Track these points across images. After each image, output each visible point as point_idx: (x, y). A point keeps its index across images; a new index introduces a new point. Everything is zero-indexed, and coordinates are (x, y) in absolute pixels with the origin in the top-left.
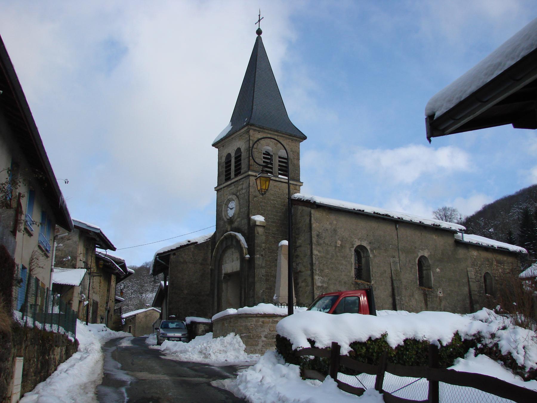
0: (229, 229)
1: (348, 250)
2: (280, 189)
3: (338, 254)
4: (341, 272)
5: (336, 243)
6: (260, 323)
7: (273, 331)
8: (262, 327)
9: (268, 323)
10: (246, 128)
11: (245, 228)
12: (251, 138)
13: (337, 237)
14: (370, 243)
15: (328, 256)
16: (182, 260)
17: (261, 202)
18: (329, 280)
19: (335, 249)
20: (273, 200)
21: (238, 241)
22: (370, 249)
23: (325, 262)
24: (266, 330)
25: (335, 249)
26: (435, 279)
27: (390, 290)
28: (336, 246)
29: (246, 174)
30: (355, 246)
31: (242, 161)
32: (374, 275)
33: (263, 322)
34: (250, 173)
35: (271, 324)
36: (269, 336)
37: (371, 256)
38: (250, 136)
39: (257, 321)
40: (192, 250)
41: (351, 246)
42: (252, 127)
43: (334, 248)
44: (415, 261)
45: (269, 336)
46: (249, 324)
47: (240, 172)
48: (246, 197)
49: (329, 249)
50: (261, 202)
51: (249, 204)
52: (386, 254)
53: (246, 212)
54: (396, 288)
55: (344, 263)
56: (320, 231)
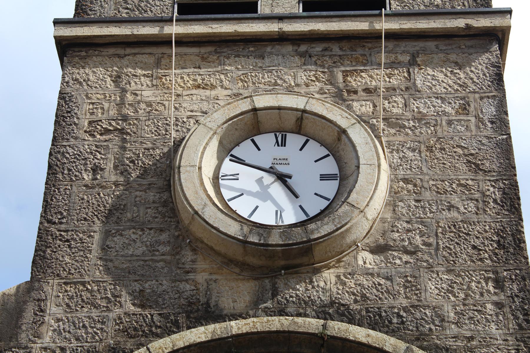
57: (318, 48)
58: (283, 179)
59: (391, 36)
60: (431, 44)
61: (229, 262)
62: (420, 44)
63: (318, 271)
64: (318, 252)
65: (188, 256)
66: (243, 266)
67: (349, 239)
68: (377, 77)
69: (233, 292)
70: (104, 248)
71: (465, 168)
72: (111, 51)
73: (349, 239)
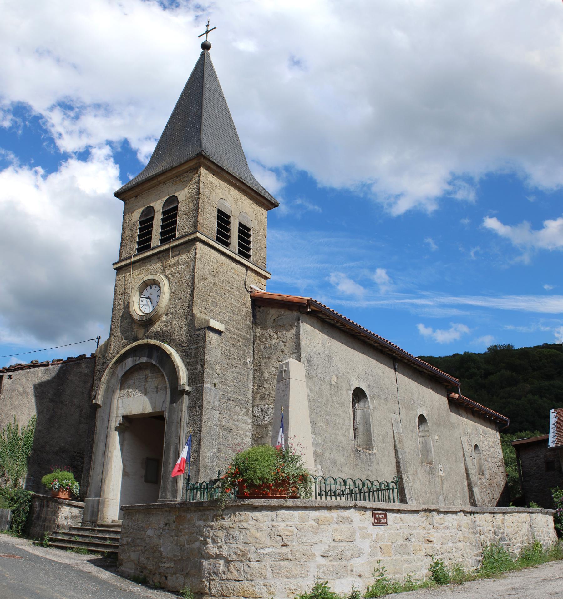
0: (140, 335)
1: (345, 392)
2: (238, 275)
3: (334, 398)
4: (339, 429)
5: (331, 378)
6: (312, 522)
7: (340, 541)
8: (316, 533)
13: (332, 369)
14: (369, 386)
15: (321, 400)
16: (21, 389)
17: (211, 290)
18: (324, 441)
19: (331, 388)
20: (229, 292)
21: (168, 357)
22: (370, 396)
23: (318, 410)
24: (324, 539)
25: (331, 388)
27: (394, 464)
28: (331, 385)
29: (192, 237)
30: (353, 388)
31: (178, 218)
32: (375, 439)
33: (318, 521)
34: (199, 235)
35: (335, 526)
36: (333, 553)
37: (371, 407)
38: (199, 177)
40: (40, 375)
41: (348, 387)
42: (206, 162)
43: (328, 387)
44: (415, 422)
45: (333, 553)
46: (282, 525)
47: (175, 236)
48: (187, 276)
49: (323, 387)
51: (193, 292)
52: (386, 407)
53: (186, 304)
54: (401, 461)
56: (312, 354)
58: (150, 299)
59: (173, 247)
60: (183, 246)
61: (140, 325)
62: (181, 247)
63: (155, 323)
64: (153, 319)
65: (133, 325)
66: (143, 326)
68: (171, 261)
69: (141, 333)
71: (185, 285)
72: (124, 269)
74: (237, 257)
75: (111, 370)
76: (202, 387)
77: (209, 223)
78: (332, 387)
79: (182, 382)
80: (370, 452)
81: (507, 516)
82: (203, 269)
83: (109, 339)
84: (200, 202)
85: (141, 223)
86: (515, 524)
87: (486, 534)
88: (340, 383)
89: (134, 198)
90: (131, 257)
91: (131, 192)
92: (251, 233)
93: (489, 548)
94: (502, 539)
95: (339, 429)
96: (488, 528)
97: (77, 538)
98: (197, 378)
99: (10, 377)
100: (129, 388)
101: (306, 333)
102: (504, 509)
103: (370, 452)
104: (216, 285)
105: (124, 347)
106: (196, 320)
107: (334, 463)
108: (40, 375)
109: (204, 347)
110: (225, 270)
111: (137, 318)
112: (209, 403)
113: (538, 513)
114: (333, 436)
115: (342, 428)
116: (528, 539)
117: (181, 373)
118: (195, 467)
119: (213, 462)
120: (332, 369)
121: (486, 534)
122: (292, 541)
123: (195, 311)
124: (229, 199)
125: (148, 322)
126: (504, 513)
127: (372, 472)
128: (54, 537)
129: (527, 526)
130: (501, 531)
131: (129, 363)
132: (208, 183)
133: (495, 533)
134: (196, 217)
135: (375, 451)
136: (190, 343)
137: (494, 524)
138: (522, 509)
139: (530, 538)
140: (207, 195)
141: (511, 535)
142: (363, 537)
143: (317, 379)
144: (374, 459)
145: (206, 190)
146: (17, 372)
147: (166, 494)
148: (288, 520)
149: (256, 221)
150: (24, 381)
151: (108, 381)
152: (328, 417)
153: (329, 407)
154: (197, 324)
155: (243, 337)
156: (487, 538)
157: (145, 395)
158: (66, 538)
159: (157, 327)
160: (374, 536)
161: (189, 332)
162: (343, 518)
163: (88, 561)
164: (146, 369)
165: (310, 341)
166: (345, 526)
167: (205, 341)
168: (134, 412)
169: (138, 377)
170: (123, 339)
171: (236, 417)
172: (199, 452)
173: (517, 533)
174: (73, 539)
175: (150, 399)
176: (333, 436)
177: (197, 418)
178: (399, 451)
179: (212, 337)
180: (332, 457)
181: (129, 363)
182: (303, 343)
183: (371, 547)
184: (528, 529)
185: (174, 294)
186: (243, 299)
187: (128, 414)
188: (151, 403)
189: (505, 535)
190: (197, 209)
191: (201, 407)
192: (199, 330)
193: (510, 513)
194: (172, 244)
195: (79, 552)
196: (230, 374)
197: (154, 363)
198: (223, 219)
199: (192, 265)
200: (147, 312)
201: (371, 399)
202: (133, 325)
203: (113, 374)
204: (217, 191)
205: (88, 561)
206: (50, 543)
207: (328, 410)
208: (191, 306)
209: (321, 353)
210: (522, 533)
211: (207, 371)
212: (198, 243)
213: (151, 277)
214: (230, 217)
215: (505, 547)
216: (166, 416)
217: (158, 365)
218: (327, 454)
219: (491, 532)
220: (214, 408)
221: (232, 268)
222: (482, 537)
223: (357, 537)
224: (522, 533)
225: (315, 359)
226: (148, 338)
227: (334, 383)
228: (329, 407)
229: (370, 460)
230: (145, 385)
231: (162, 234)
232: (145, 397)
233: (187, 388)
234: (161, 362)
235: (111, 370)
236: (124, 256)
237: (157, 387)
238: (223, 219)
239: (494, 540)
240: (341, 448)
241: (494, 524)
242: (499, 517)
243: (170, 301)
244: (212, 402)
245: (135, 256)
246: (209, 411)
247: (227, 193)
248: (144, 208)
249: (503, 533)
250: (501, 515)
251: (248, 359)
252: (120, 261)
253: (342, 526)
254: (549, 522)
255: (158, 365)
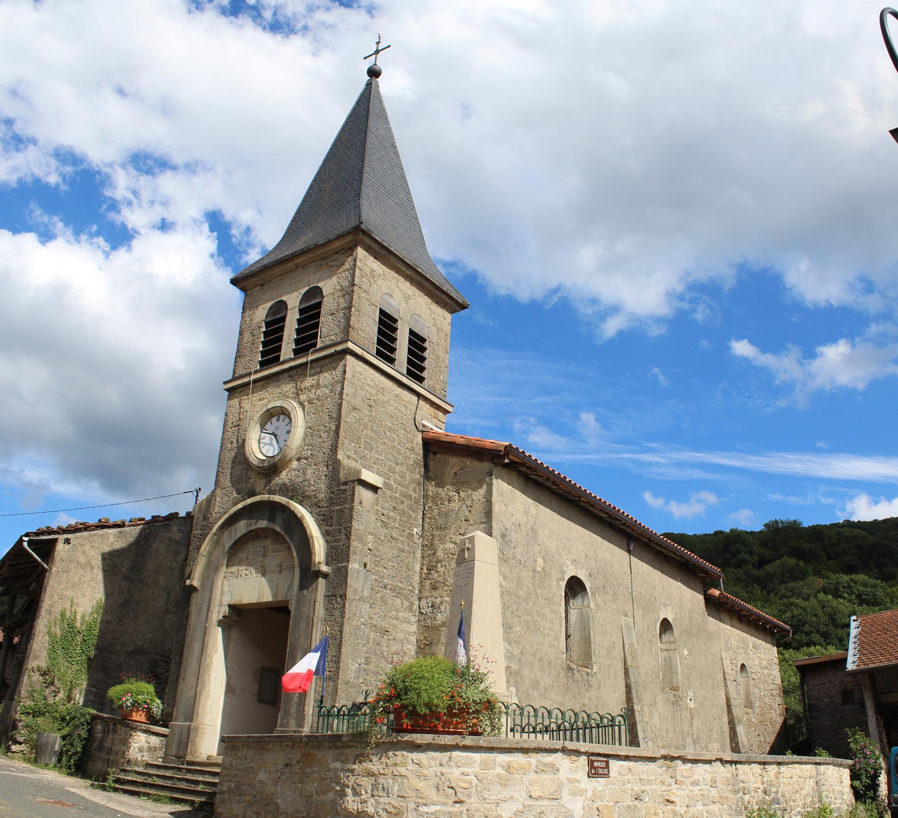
0: (258, 489)
1: (554, 583)
2: (405, 406)
3: (539, 591)
4: (544, 637)
6: (499, 770)
9: (525, 771)
10: (349, 239)
11: (319, 486)
12: (358, 263)
13: (537, 548)
16: (82, 560)
18: (522, 653)
20: (391, 430)
21: (298, 522)
22: (591, 589)
23: (515, 607)
24: (516, 795)
26: (683, 672)
27: (623, 689)
30: (567, 577)
33: (508, 768)
34: (350, 345)
35: (534, 776)
37: (592, 605)
38: (355, 260)
39: (485, 765)
41: (560, 576)
42: (366, 239)
43: (531, 574)
44: (655, 630)
47: (315, 345)
48: (330, 405)
49: (523, 574)
50: (365, 426)
52: (615, 606)
53: (328, 444)
54: (633, 685)
55: (549, 614)
56: (508, 526)
57: (294, 372)
58: (275, 436)
59: (313, 361)
60: (327, 361)
61: (259, 473)
62: (323, 362)
64: (279, 466)
65: (250, 472)
66: (263, 474)
67: (288, 458)
68: (309, 381)
69: (260, 485)
70: (231, 473)
71: (327, 418)
73: (288, 458)
74: (405, 380)
75: (215, 537)
76: (346, 568)
77: (367, 329)
78: (537, 575)
79: (317, 560)
80: (589, 671)
81: (783, 768)
82: (354, 395)
83: (214, 492)
84: (355, 297)
85: (268, 324)
86: (794, 779)
87: (753, 794)
88: (547, 569)
89: (258, 288)
90: (250, 374)
91: (255, 279)
92: (426, 345)
93: (755, 814)
94: (776, 801)
95: (544, 637)
96: (756, 785)
97: (155, 779)
98: (339, 553)
99: (67, 541)
100: (239, 564)
101: (501, 494)
102: (780, 758)
103: (589, 671)
104: (372, 419)
105: (235, 504)
106: (341, 469)
107: (535, 685)
108: (111, 540)
109: (352, 509)
110: (386, 399)
111: (255, 462)
112: (355, 591)
113: (828, 764)
114: (535, 646)
115: (548, 635)
116: (813, 802)
117: (316, 546)
118: (331, 683)
119: (358, 677)
120: (537, 548)
121: (753, 794)
122: (469, 796)
123: (340, 457)
124: (397, 294)
125: (272, 469)
126: (779, 764)
127: (590, 699)
128: (122, 776)
129: (811, 782)
130: (774, 789)
131: (242, 527)
132: (367, 270)
133: (765, 792)
134: (348, 319)
135: (595, 670)
136: (331, 502)
137: (765, 779)
138: (805, 758)
139: (816, 799)
140: (365, 287)
141: (788, 796)
142: (574, 794)
143: (514, 562)
144: (593, 681)
145: (364, 280)
146: (79, 534)
147: (288, 722)
148: (465, 765)
149: (434, 329)
150: (87, 547)
151: (210, 554)
152: (529, 618)
153: (531, 603)
154: (342, 476)
155: (409, 497)
156: (754, 800)
157: (263, 575)
158: (140, 779)
159: (284, 477)
160: (590, 793)
161: (329, 487)
162: (545, 765)
163: (171, 813)
164: (266, 537)
165: (506, 506)
166: (547, 777)
167: (353, 501)
168: (246, 601)
169: (253, 548)
170: (234, 492)
171: (394, 613)
172: (339, 662)
173: (797, 792)
174: (149, 781)
175: (270, 582)
176: (535, 646)
177: (337, 613)
178: (630, 670)
179: (363, 494)
180: (532, 676)
181: (242, 527)
182: (496, 508)
183: (584, 808)
184: (813, 787)
185: (310, 430)
186: (411, 442)
187: (237, 603)
188: (271, 588)
189: (780, 795)
190: (349, 308)
191: (343, 596)
192: (345, 483)
193: (788, 763)
194: (311, 357)
195: (157, 799)
196: (387, 551)
197: (278, 529)
198: (387, 324)
199: (339, 389)
200: (271, 455)
201: (593, 594)
202: (250, 472)
203: (217, 543)
204: (380, 282)
205: (171, 813)
206: (117, 786)
207: (529, 607)
208: (334, 449)
209: (522, 524)
210: (804, 792)
211: (355, 544)
212: (348, 357)
213: (278, 403)
214: (395, 321)
215: (779, 813)
216: (292, 608)
217: (283, 533)
218: (526, 671)
219: (760, 791)
220: (362, 599)
221: (397, 396)
222: (747, 798)
223: (565, 793)
224: (804, 792)
225: (513, 533)
226: (271, 492)
227: (539, 569)
228: (531, 603)
229: (588, 682)
230: (263, 561)
231: (297, 342)
232: (263, 578)
233: (324, 568)
234: (287, 529)
235: (215, 537)
236: (240, 371)
237: (280, 566)
238: (387, 324)
239: (764, 801)
240: (546, 664)
241: (765, 779)
242: (773, 769)
243: (304, 439)
244: (360, 590)
245: (256, 372)
246: (354, 603)
247: (393, 286)
248: (272, 303)
249: (777, 792)
250: (775, 766)
251: (415, 530)
252: (234, 379)
253: (543, 776)
254: (843, 778)
255: (283, 533)
